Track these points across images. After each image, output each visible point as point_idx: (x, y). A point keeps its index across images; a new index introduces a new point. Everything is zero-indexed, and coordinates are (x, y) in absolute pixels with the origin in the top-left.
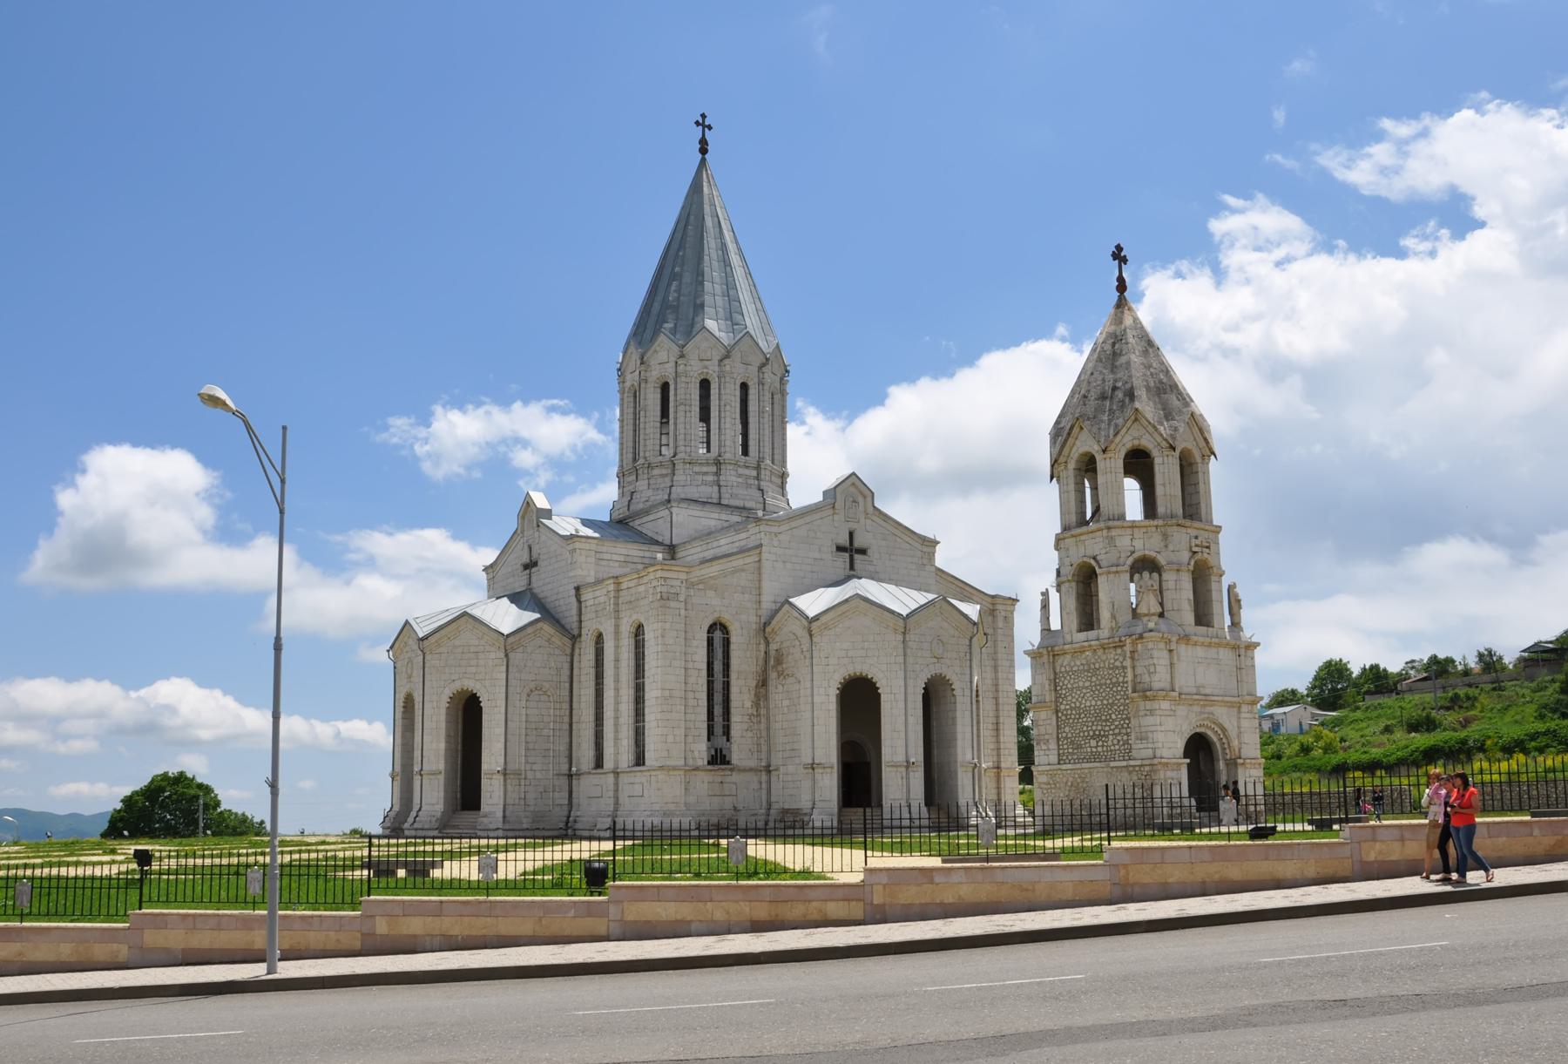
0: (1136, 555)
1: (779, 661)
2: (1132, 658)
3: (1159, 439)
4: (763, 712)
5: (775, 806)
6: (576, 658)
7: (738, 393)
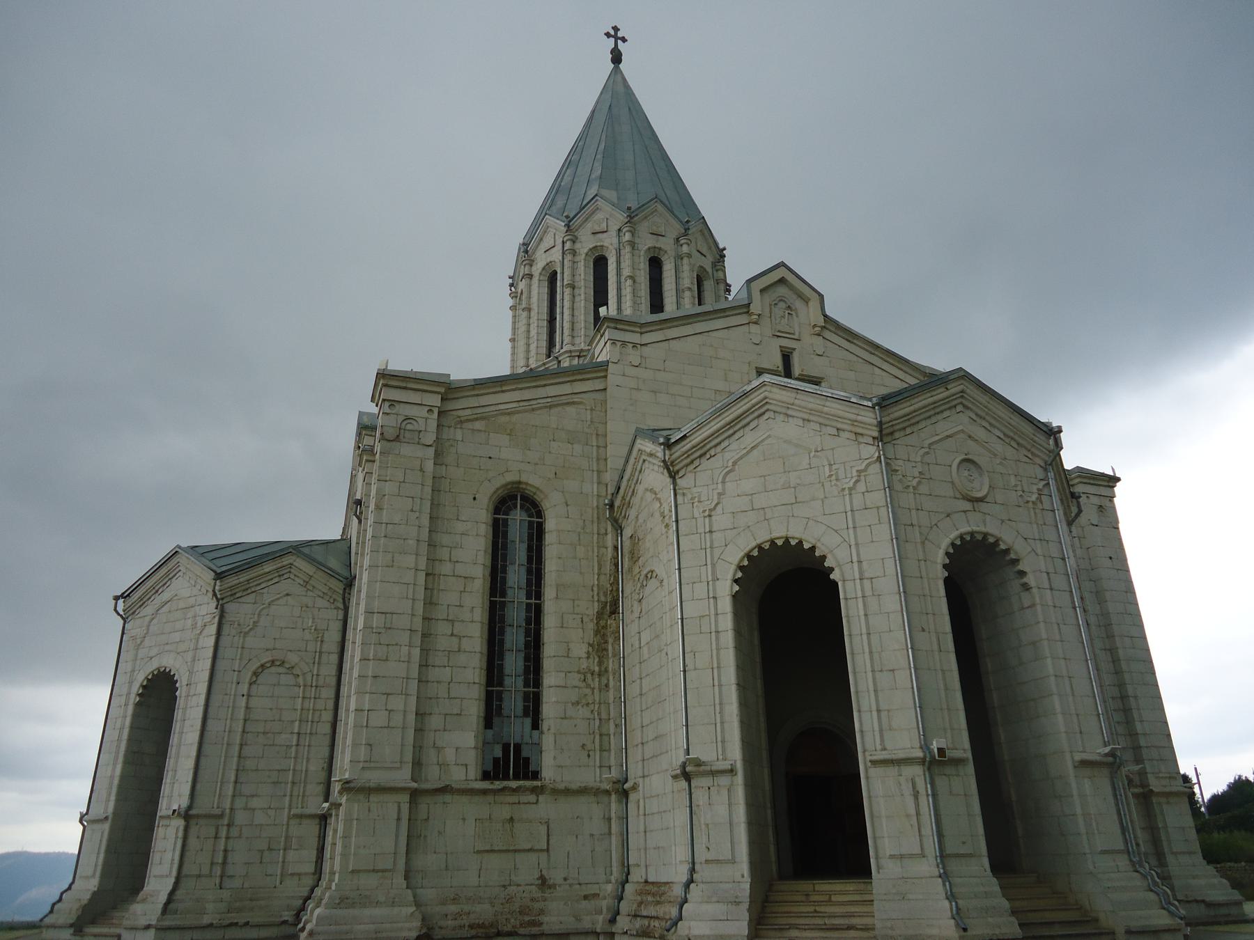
1: (634, 558)
5: (636, 876)
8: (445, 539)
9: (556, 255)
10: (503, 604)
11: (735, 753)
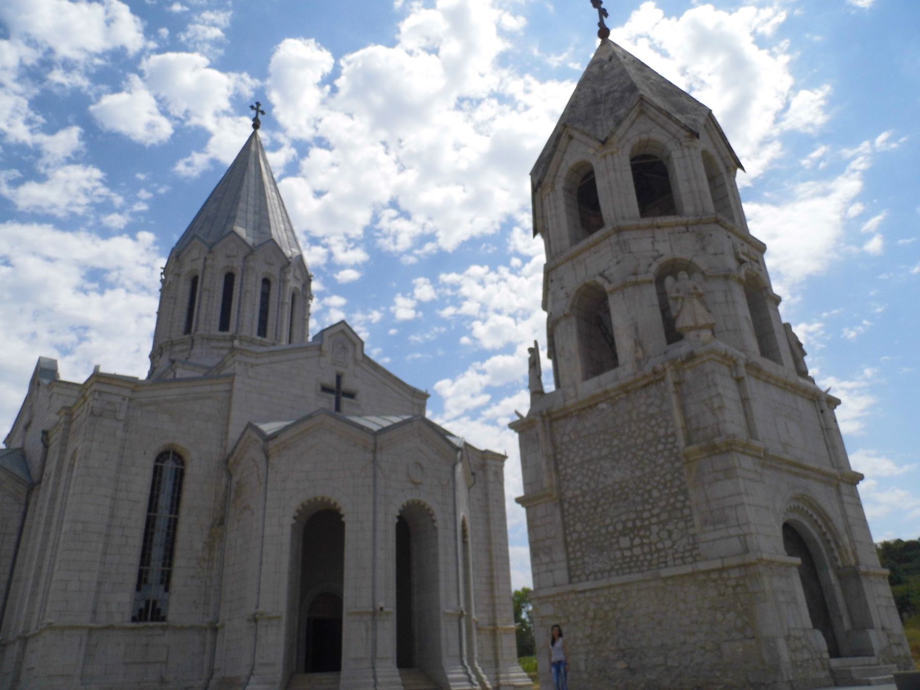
0: (662, 260)
2: (681, 396)
3: (674, 128)
6: (31, 506)
9: (199, 265)
10: (155, 517)
11: (282, 608)
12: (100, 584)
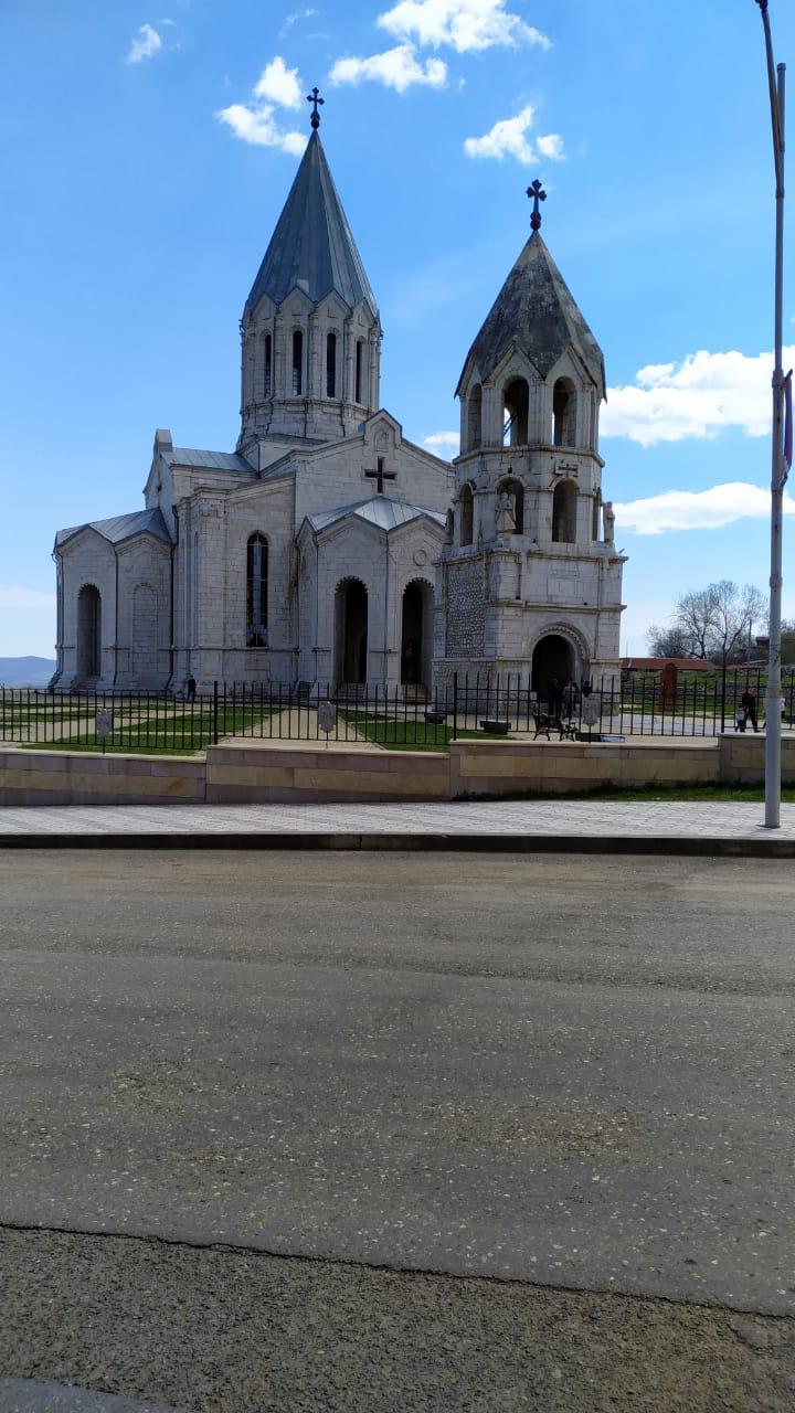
0: (502, 478)
1: (304, 568)
4: (294, 605)
7: (325, 343)
8: (228, 556)
12: (225, 624)
